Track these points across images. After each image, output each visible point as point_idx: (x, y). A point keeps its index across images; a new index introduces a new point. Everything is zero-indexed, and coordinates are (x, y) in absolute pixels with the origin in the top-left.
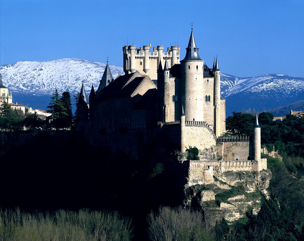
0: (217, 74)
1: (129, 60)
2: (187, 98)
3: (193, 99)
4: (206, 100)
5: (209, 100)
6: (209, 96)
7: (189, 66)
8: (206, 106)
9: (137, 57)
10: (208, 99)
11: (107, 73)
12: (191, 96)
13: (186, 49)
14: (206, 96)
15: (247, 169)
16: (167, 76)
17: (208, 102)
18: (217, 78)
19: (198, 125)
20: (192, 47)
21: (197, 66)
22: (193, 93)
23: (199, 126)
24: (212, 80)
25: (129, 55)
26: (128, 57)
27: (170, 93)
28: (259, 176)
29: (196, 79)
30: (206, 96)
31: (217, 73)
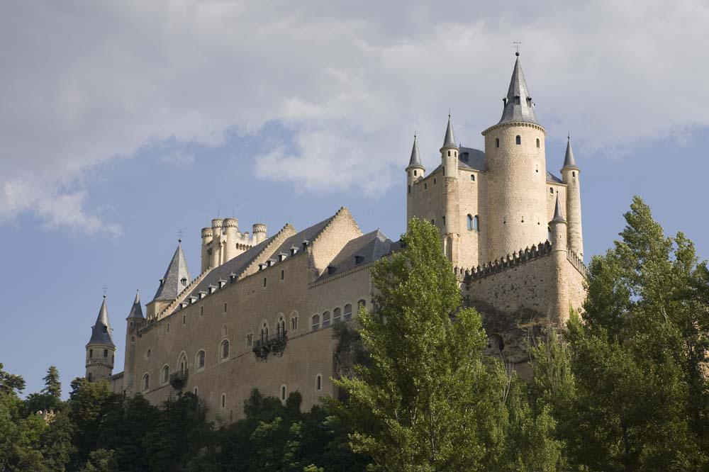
0: (574, 176)
1: (222, 248)
2: (514, 217)
7: (518, 138)
9: (239, 243)
11: (180, 264)
12: (526, 213)
16: (455, 161)
18: (575, 185)
24: (562, 189)
25: (224, 238)
26: (221, 241)
27: (461, 207)
29: (537, 171)
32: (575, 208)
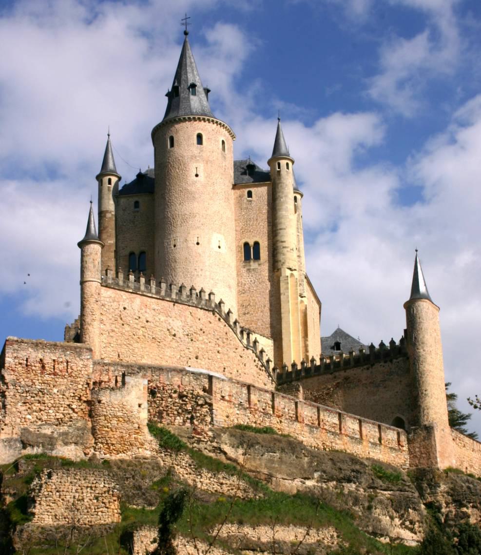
0: (279, 167)
3: (186, 240)
4: (247, 258)
5: (257, 257)
6: (257, 244)
7: (172, 139)
8: (247, 279)
10: (250, 252)
13: (166, 95)
14: (246, 245)
15: (381, 455)
17: (254, 265)
18: (280, 179)
19: (174, 296)
20: (183, 82)
21: (200, 137)
22: (185, 220)
23: (175, 302)
28: (443, 487)
29: (197, 175)
30: (246, 245)
31: (279, 164)
32: (280, 210)
